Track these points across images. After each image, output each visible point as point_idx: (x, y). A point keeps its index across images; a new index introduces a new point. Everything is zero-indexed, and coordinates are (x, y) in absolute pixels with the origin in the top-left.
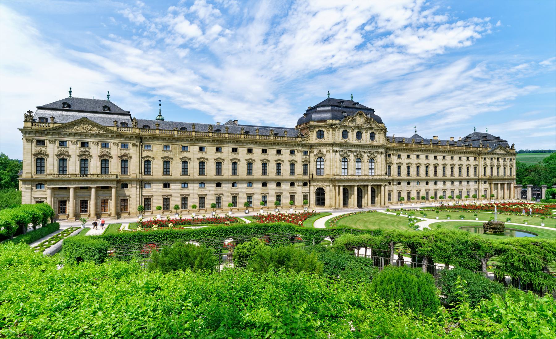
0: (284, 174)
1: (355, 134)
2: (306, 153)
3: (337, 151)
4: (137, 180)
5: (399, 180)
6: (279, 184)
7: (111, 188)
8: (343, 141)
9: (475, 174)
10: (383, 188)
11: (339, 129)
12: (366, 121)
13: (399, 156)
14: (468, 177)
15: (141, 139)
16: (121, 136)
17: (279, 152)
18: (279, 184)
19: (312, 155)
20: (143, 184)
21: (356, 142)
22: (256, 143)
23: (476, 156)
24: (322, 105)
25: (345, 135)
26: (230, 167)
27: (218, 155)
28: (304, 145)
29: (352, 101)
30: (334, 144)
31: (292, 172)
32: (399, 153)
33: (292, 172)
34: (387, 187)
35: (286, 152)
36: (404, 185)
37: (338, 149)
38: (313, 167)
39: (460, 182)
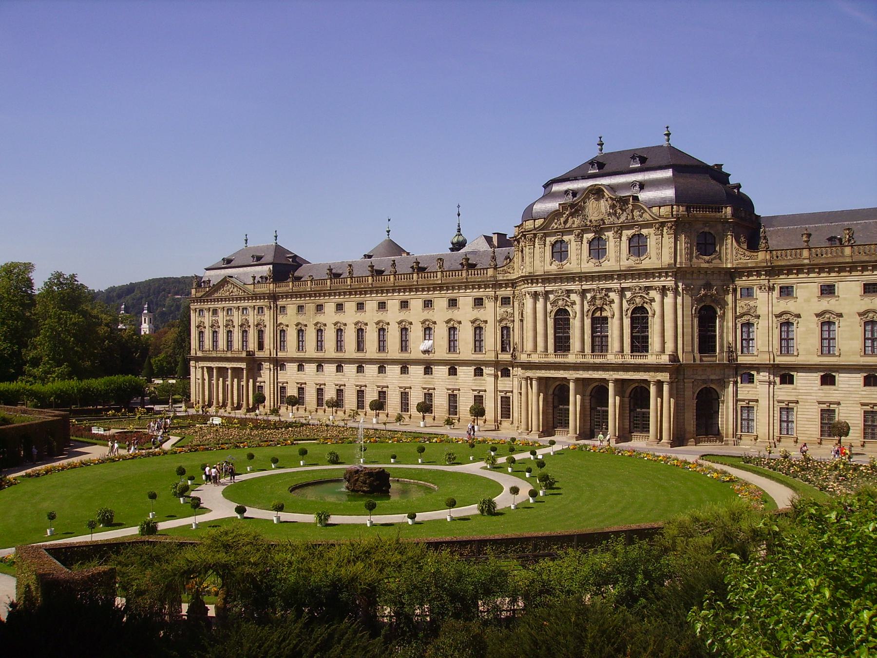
1: (585, 246)
2: (506, 301)
3: (535, 295)
4: (270, 360)
6: (453, 372)
7: (243, 369)
8: (554, 268)
10: (653, 390)
12: (613, 207)
13: (786, 292)
15: (274, 297)
16: (255, 297)
17: (453, 303)
18: (453, 372)
19: (516, 304)
20: (279, 364)
21: (589, 266)
22: (410, 289)
25: (560, 252)
26: (376, 335)
28: (497, 285)
30: (531, 279)
31: (478, 343)
32: (784, 280)
33: (478, 343)
34: (666, 388)
35: (466, 299)
36: (807, 385)
37: (539, 288)
38: (516, 337)
39: (320, 367)
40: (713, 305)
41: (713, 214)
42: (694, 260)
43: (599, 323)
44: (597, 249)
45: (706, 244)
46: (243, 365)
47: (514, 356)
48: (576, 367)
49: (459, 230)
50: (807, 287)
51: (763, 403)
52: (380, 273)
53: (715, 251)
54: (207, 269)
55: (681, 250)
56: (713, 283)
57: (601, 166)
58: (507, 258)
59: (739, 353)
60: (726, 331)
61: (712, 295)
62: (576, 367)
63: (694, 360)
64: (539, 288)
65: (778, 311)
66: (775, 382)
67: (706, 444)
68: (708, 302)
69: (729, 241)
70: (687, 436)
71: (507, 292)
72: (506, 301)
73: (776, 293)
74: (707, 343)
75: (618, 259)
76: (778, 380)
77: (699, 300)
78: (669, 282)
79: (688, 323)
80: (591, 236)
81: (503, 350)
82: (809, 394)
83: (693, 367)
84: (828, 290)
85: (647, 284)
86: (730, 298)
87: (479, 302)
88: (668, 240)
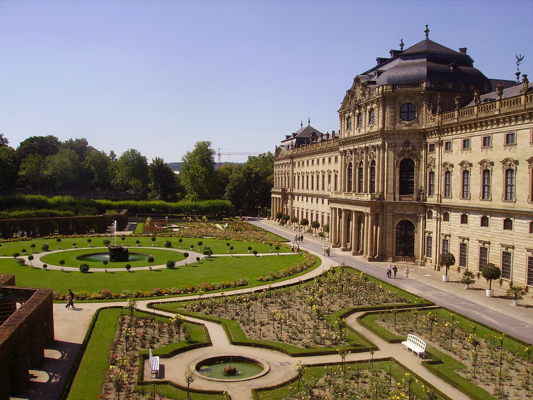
21: (357, 133)
29: (428, 41)
40: (411, 158)
41: (414, 89)
42: (398, 125)
45: (408, 112)
46: (280, 196)
50: (456, 142)
53: (415, 117)
54: (282, 142)
55: (387, 118)
56: (411, 141)
59: (427, 195)
60: (420, 180)
61: (409, 151)
63: (395, 199)
66: (441, 219)
67: (403, 262)
68: (407, 156)
69: (424, 109)
70: (388, 255)
73: (444, 147)
74: (406, 185)
76: (442, 216)
77: (400, 155)
79: (391, 171)
80: (357, 111)
82: (455, 230)
83: (394, 205)
85: (373, 144)
86: (423, 153)
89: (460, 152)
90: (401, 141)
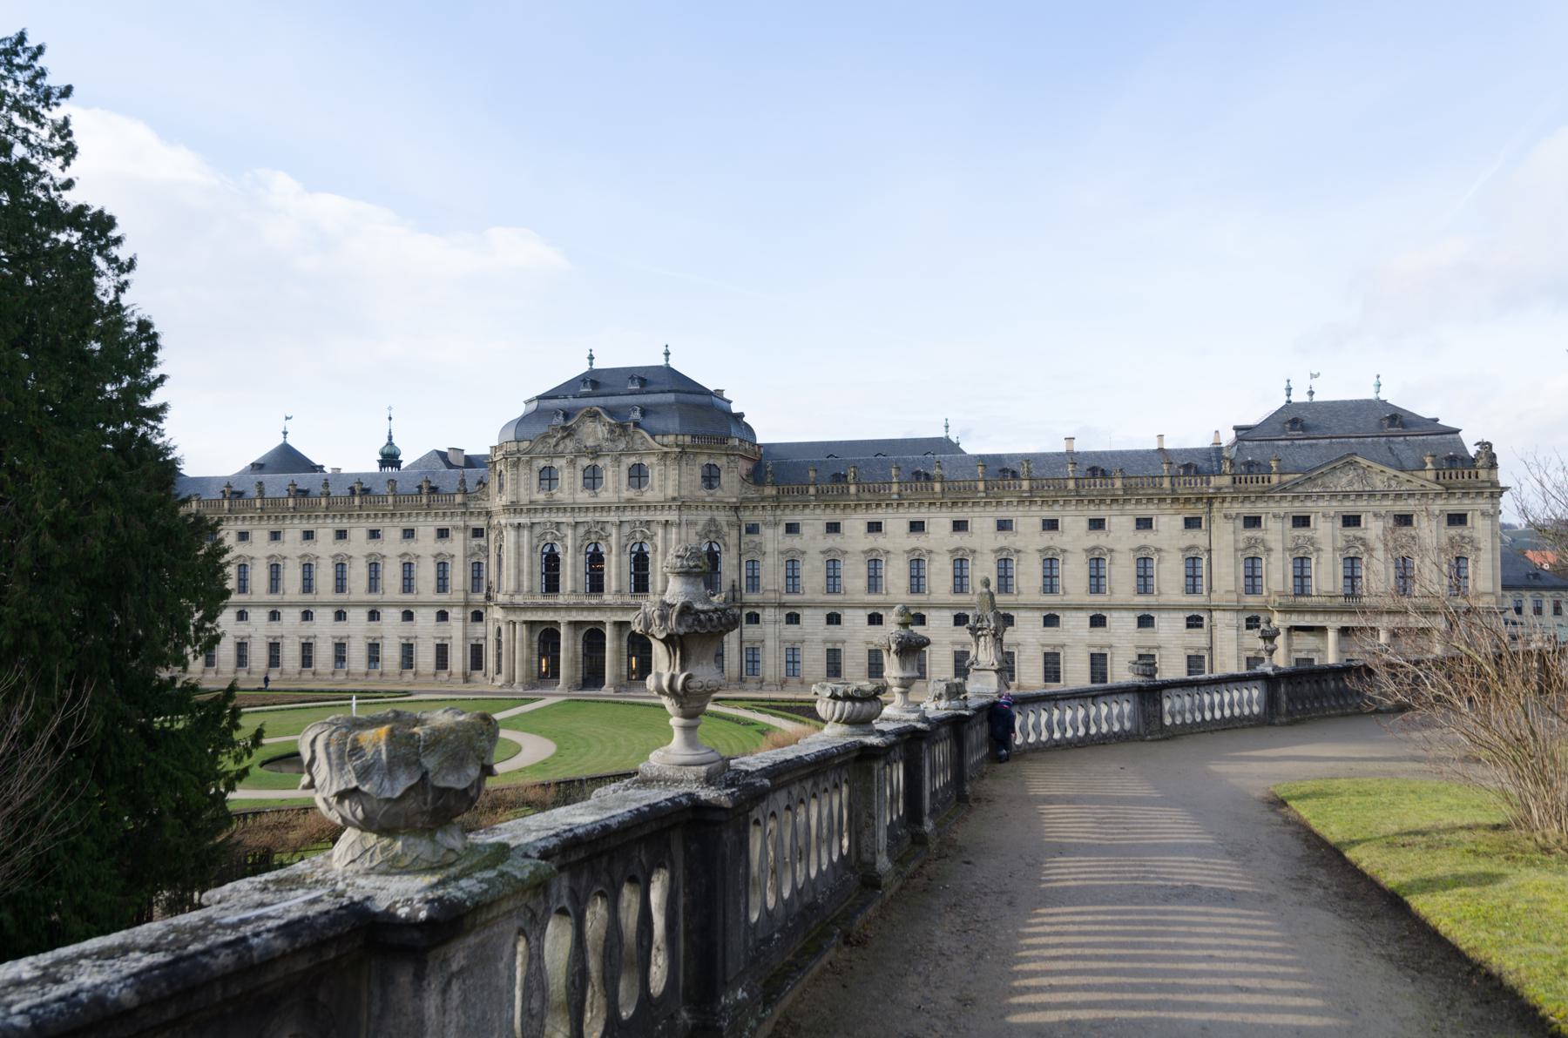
0: (421, 588)
1: (580, 474)
5: (781, 606)
8: (541, 497)
9: (1192, 589)
11: (529, 462)
12: (611, 432)
13: (792, 529)
14: (1142, 600)
19: (492, 537)
21: (584, 497)
23: (1198, 510)
24: (531, 401)
25: (548, 477)
27: (275, 548)
37: (524, 520)
43: (596, 559)
44: (592, 479)
47: (488, 598)
48: (568, 608)
49: (390, 438)
51: (770, 643)
52: (305, 493)
57: (595, 384)
58: (480, 483)
62: (568, 608)
64: (524, 520)
65: (784, 547)
71: (479, 523)
72: (478, 533)
73: (782, 529)
75: (617, 491)
78: (672, 516)
80: (586, 462)
81: (476, 587)
84: (833, 528)
87: (443, 533)
88: (673, 473)
89: (820, 538)
90: (702, 518)
